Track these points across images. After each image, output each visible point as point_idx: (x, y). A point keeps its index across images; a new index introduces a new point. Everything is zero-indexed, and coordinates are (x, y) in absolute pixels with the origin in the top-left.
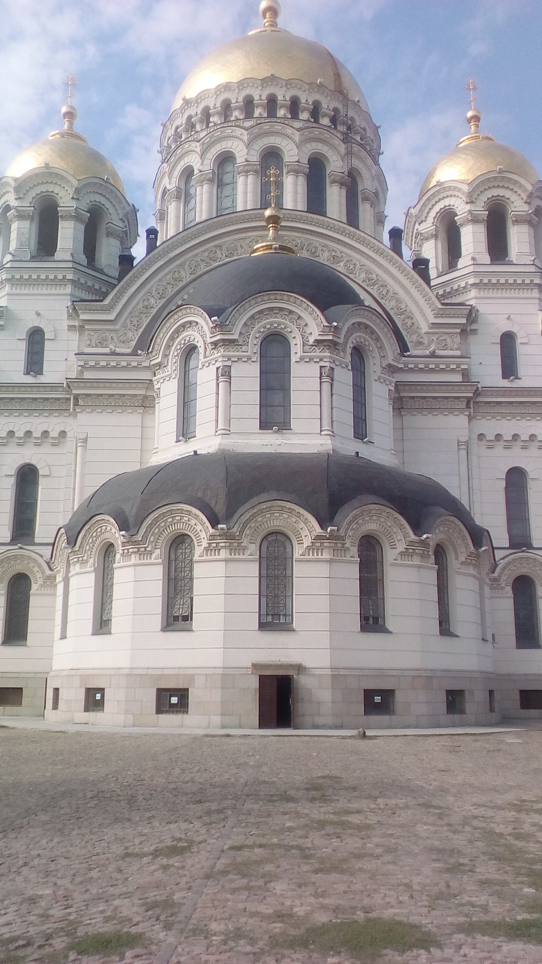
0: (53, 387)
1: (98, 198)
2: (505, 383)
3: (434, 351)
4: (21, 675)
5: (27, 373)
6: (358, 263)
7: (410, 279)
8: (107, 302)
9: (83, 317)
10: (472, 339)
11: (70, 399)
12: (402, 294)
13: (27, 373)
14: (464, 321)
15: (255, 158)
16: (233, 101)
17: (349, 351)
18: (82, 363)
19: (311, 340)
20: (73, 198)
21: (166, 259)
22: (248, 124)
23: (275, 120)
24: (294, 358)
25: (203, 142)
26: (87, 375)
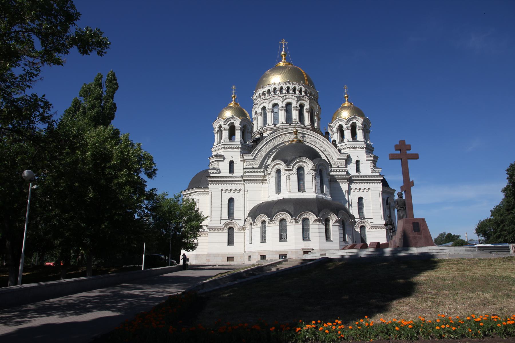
0: (239, 177)
1: (246, 124)
2: (357, 174)
3: (338, 166)
4: (233, 254)
6: (317, 142)
7: (332, 147)
8: (251, 154)
9: (245, 158)
11: (242, 180)
12: (329, 150)
13: (230, 173)
14: (346, 158)
15: (284, 105)
16: (277, 88)
17: (319, 171)
18: (245, 171)
19: (310, 169)
20: (239, 124)
21: (266, 142)
22: (282, 95)
23: (289, 94)
24: (306, 173)
25: (269, 101)
26: (247, 174)
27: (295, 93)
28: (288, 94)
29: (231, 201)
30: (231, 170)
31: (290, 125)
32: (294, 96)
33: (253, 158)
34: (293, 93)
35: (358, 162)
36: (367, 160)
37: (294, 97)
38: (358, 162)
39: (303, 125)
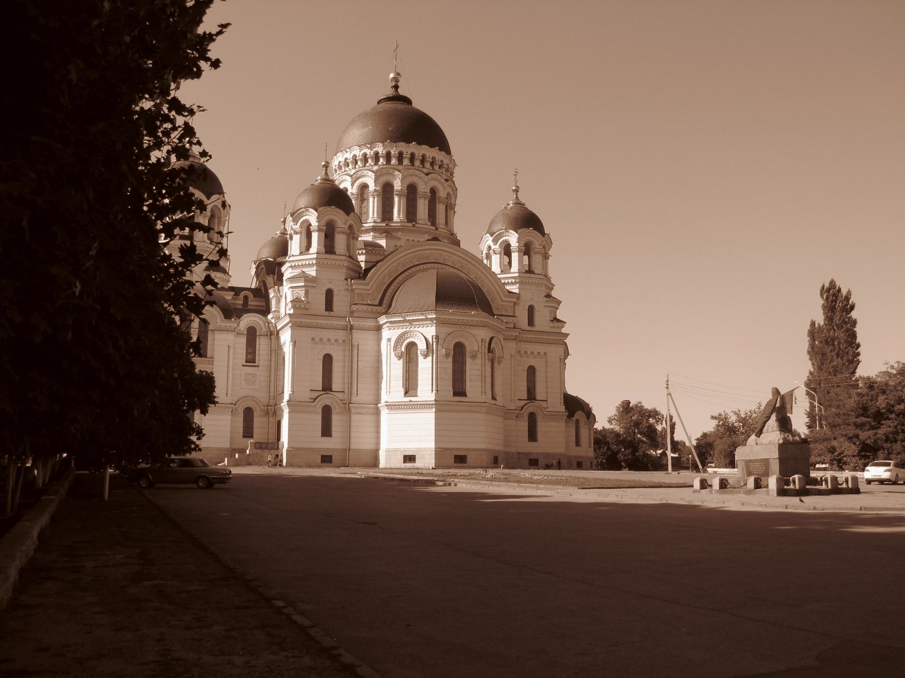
5: (326, 310)
10: (517, 307)
13: (326, 310)
14: (515, 300)
22: (400, 167)
23: (414, 168)
27: (423, 167)
28: (412, 167)
29: (328, 360)
30: (329, 306)
31: (414, 226)
32: (423, 172)
33: (369, 288)
34: (421, 166)
35: (531, 309)
36: (546, 306)
37: (423, 175)
38: (531, 309)
39: (434, 228)
